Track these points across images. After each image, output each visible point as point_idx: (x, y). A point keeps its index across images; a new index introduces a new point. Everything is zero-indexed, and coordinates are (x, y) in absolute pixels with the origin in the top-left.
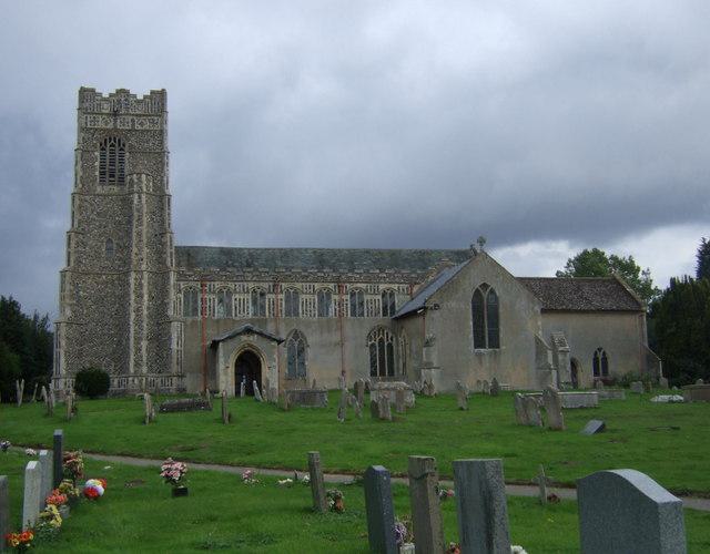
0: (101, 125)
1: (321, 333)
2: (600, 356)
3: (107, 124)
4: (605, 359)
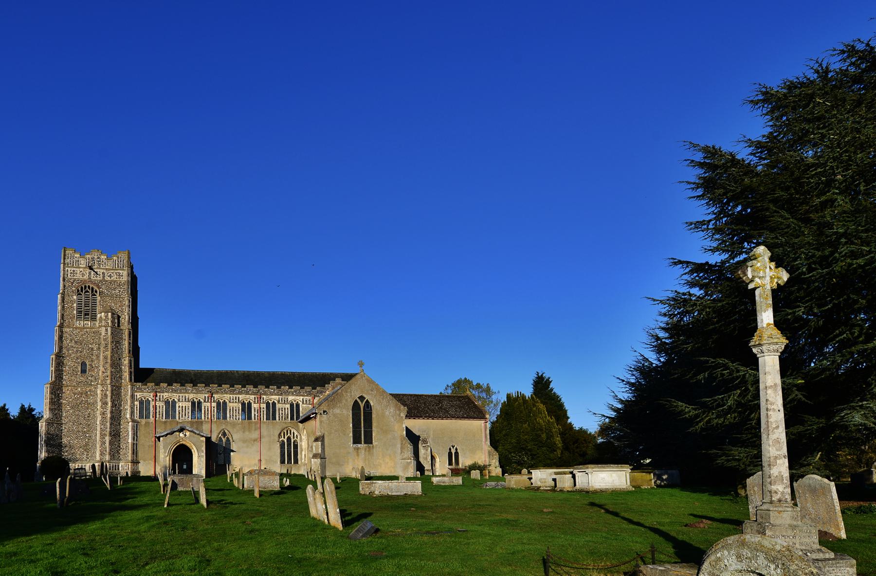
0: (79, 276)
1: (244, 432)
2: (453, 451)
3: (83, 275)
4: (457, 454)
